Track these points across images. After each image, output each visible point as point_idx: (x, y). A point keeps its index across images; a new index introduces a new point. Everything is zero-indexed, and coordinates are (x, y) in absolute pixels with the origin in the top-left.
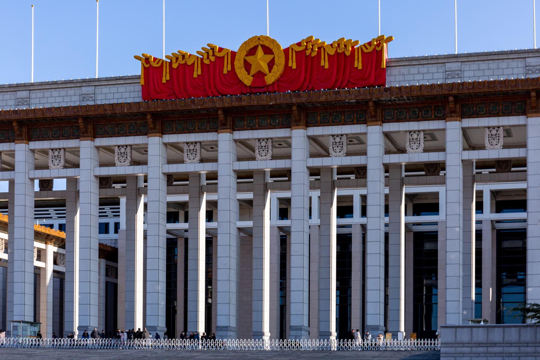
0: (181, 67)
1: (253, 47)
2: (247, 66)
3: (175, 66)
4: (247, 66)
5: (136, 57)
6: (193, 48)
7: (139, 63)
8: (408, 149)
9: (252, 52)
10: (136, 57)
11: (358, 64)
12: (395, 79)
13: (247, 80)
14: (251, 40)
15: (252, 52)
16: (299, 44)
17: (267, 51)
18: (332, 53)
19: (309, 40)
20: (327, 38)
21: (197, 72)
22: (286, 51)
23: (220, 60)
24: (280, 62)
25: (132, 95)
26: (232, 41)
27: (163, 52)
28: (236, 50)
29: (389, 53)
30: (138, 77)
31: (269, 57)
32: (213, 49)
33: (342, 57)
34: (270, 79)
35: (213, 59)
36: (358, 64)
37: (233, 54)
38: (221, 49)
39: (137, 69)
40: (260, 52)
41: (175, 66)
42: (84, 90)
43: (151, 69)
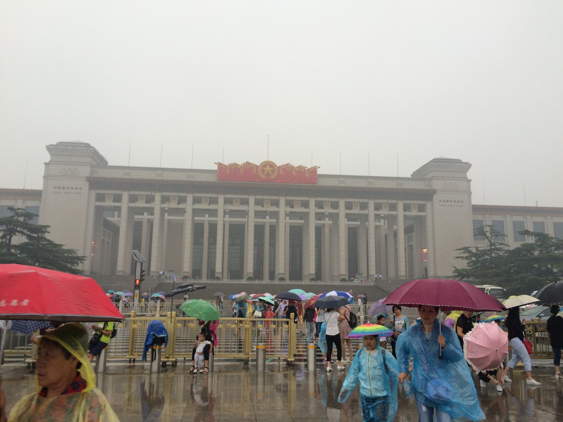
0: (234, 168)
3: (232, 168)
4: (263, 171)
5: (216, 163)
6: (240, 162)
8: (324, 207)
10: (216, 163)
12: (322, 183)
13: (263, 177)
16: (284, 165)
18: (297, 170)
19: (288, 164)
22: (279, 167)
25: (212, 178)
27: (227, 162)
28: (258, 164)
29: (319, 172)
30: (216, 171)
32: (248, 163)
34: (273, 177)
35: (248, 167)
38: (252, 164)
39: (215, 168)
41: (232, 168)
42: (189, 173)
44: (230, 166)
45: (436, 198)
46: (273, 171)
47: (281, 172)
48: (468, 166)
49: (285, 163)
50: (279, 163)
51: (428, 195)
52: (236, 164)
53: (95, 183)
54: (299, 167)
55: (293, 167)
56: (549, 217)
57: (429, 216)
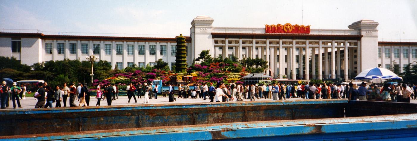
1: (287, 25)
2: (286, 28)
3: (272, 27)
4: (286, 28)
6: (276, 24)
7: (265, 26)
9: (287, 26)
11: (305, 29)
13: (286, 31)
14: (286, 24)
15: (287, 26)
16: (295, 25)
17: (289, 26)
18: (301, 27)
20: (300, 24)
21: (277, 28)
22: (293, 26)
23: (281, 27)
24: (292, 27)
26: (283, 23)
29: (311, 28)
31: (290, 27)
33: (303, 28)
34: (290, 31)
36: (305, 29)
37: (283, 26)
38: (281, 25)
39: (265, 27)
40: (288, 26)
43: (267, 27)
44: (271, 26)
45: (362, 39)
46: (290, 28)
47: (294, 28)
48: (377, 25)
49: (295, 24)
50: (293, 24)
51: (359, 38)
52: (274, 25)
53: (214, 36)
54: (302, 26)
55: (299, 26)
56: (410, 47)
57: (359, 47)
